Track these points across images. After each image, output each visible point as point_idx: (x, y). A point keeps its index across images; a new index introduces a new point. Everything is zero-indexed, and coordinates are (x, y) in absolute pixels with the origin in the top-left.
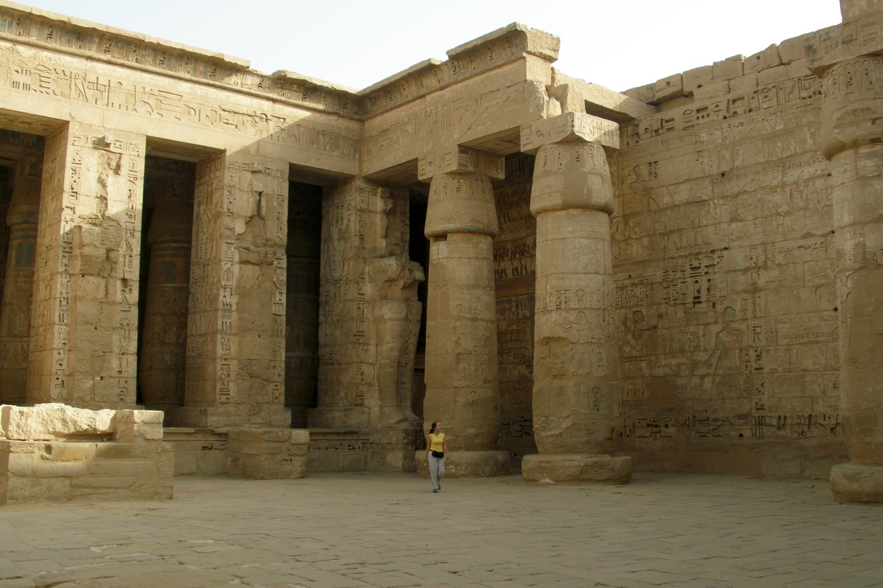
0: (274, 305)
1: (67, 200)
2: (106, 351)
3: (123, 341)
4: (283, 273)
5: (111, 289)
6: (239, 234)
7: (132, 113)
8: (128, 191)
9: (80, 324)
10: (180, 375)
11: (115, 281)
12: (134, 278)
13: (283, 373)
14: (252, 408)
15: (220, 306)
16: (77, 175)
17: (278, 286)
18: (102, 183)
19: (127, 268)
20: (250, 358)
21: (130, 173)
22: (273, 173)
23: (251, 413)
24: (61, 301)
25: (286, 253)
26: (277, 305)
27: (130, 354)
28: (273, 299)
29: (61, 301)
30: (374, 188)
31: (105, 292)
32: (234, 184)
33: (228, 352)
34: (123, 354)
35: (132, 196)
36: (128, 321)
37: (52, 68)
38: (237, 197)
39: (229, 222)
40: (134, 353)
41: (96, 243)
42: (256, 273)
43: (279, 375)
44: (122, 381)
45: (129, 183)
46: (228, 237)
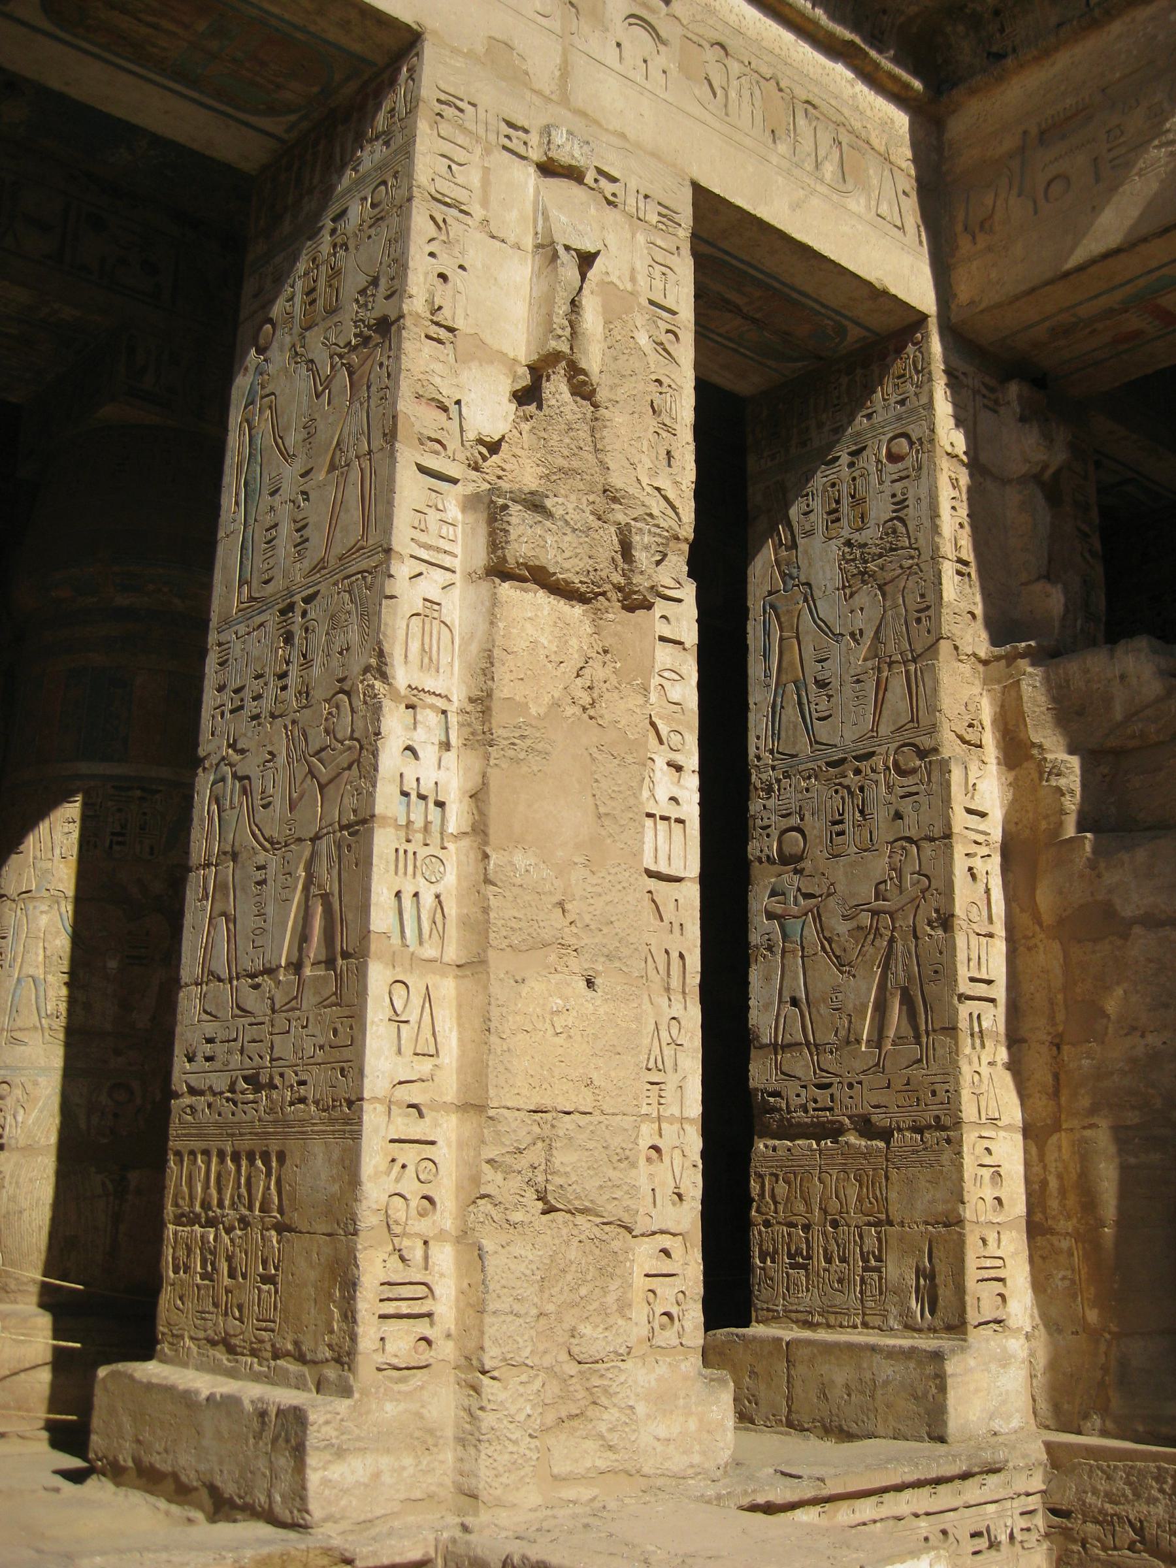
4: (684, 671)
6: (480, 441)
10: (134, 1177)
13: (693, 1184)
14: (554, 1388)
15: (386, 801)
17: (664, 729)
20: (547, 1102)
22: (631, 201)
23: (550, 1418)
25: (690, 575)
26: (662, 825)
30: (987, 379)
33: (425, 1067)
38: (472, 258)
39: (438, 367)
42: (574, 642)
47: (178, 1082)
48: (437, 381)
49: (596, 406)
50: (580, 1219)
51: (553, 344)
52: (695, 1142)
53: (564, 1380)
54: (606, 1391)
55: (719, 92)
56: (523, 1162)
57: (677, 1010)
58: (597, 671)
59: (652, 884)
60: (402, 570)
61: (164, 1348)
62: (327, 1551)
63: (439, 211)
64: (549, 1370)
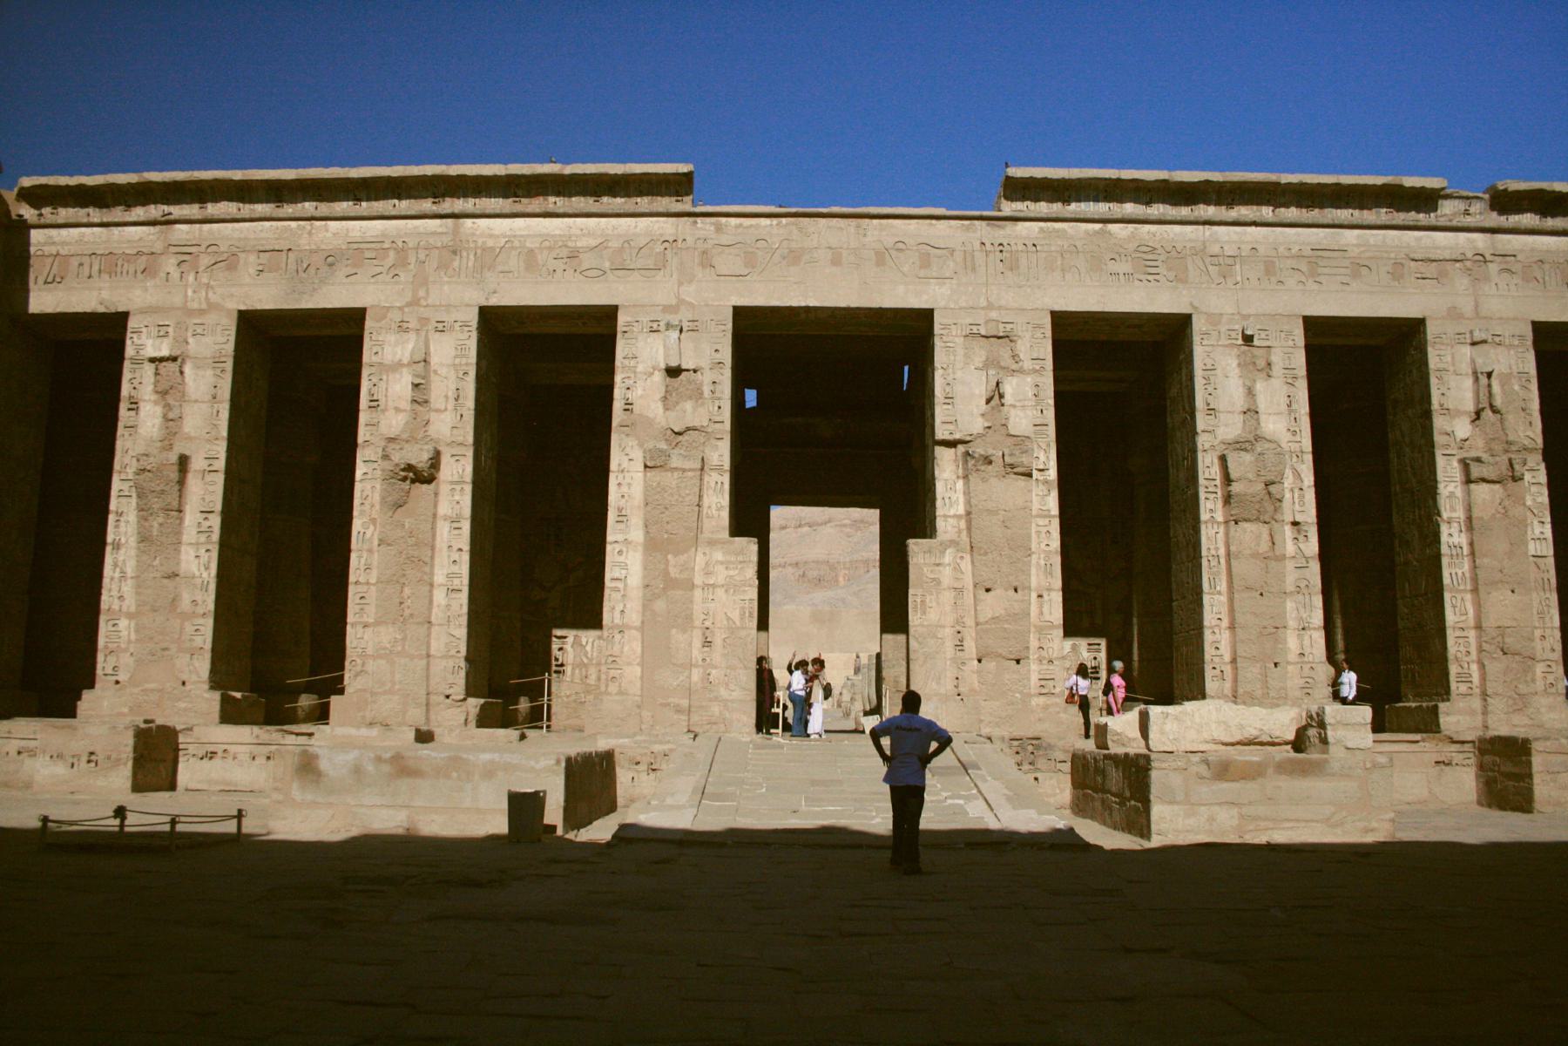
0: (1533, 541)
1: (1201, 422)
2: (1278, 626)
3: (1302, 610)
5: (1277, 539)
6: (1462, 440)
7: (1277, 287)
8: (1286, 398)
9: (1238, 590)
11: (1283, 526)
12: (1310, 520)
13: (1559, 647)
14: (1511, 702)
15: (1444, 549)
16: (1212, 385)
18: (1250, 392)
19: (1297, 507)
21: (1286, 371)
22: (1507, 341)
24: (1209, 561)
25: (1544, 460)
26: (1538, 542)
27: (1315, 629)
28: (1529, 533)
29: (1209, 561)
31: (1270, 544)
32: (1445, 366)
33: (1464, 618)
34: (1303, 629)
35: (1293, 405)
36: (1306, 583)
37: (1158, 246)
38: (1452, 384)
39: (1444, 423)
40: (1319, 627)
41: (1250, 476)
43: (1553, 650)
44: (1306, 668)
45: (1285, 387)
46: (1447, 446)
47: (1400, 627)
48: (1445, 427)
49: (1501, 414)
50: (1516, 657)
51: (1481, 406)
52: (1558, 634)
53: (1514, 699)
54: (1529, 703)
55: (1541, 280)
56: (1496, 641)
57: (1548, 595)
58: (1506, 503)
59: (1535, 559)
60: (1441, 486)
61: (1404, 699)
62: (1445, 736)
63: (1438, 374)
64: (1510, 697)
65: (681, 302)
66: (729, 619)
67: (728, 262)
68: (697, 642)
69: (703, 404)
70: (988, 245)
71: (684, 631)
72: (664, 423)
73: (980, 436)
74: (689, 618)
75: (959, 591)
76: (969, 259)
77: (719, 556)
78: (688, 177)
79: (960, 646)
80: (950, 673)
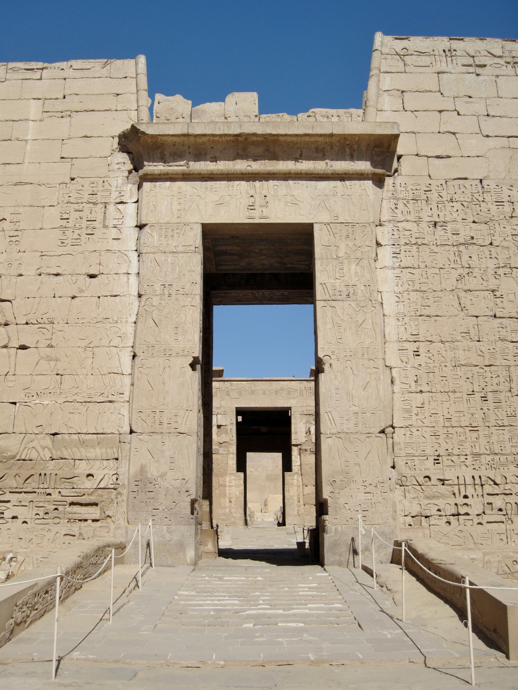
65: (221, 406)
66: (236, 495)
67: (234, 395)
68: (227, 501)
69: (228, 435)
70: (307, 388)
71: (224, 498)
72: (217, 441)
73: (304, 443)
74: (225, 495)
75: (299, 486)
76: (301, 392)
77: (233, 478)
78: (222, 371)
79: (299, 501)
80: (296, 509)
